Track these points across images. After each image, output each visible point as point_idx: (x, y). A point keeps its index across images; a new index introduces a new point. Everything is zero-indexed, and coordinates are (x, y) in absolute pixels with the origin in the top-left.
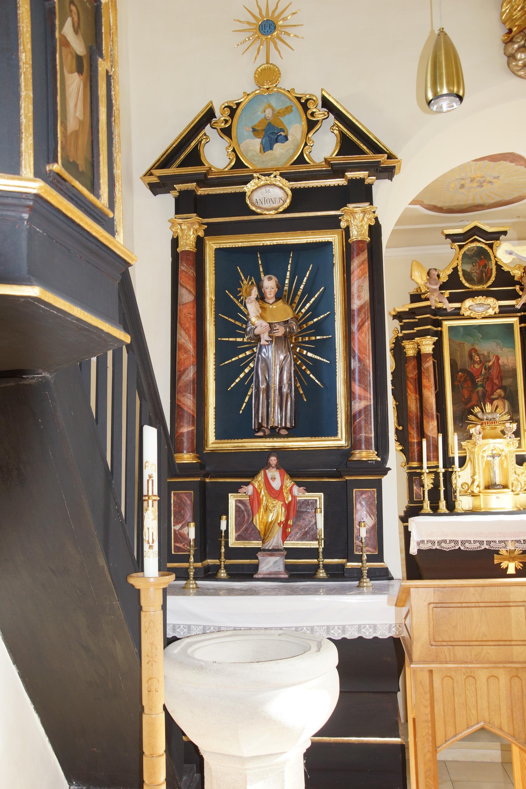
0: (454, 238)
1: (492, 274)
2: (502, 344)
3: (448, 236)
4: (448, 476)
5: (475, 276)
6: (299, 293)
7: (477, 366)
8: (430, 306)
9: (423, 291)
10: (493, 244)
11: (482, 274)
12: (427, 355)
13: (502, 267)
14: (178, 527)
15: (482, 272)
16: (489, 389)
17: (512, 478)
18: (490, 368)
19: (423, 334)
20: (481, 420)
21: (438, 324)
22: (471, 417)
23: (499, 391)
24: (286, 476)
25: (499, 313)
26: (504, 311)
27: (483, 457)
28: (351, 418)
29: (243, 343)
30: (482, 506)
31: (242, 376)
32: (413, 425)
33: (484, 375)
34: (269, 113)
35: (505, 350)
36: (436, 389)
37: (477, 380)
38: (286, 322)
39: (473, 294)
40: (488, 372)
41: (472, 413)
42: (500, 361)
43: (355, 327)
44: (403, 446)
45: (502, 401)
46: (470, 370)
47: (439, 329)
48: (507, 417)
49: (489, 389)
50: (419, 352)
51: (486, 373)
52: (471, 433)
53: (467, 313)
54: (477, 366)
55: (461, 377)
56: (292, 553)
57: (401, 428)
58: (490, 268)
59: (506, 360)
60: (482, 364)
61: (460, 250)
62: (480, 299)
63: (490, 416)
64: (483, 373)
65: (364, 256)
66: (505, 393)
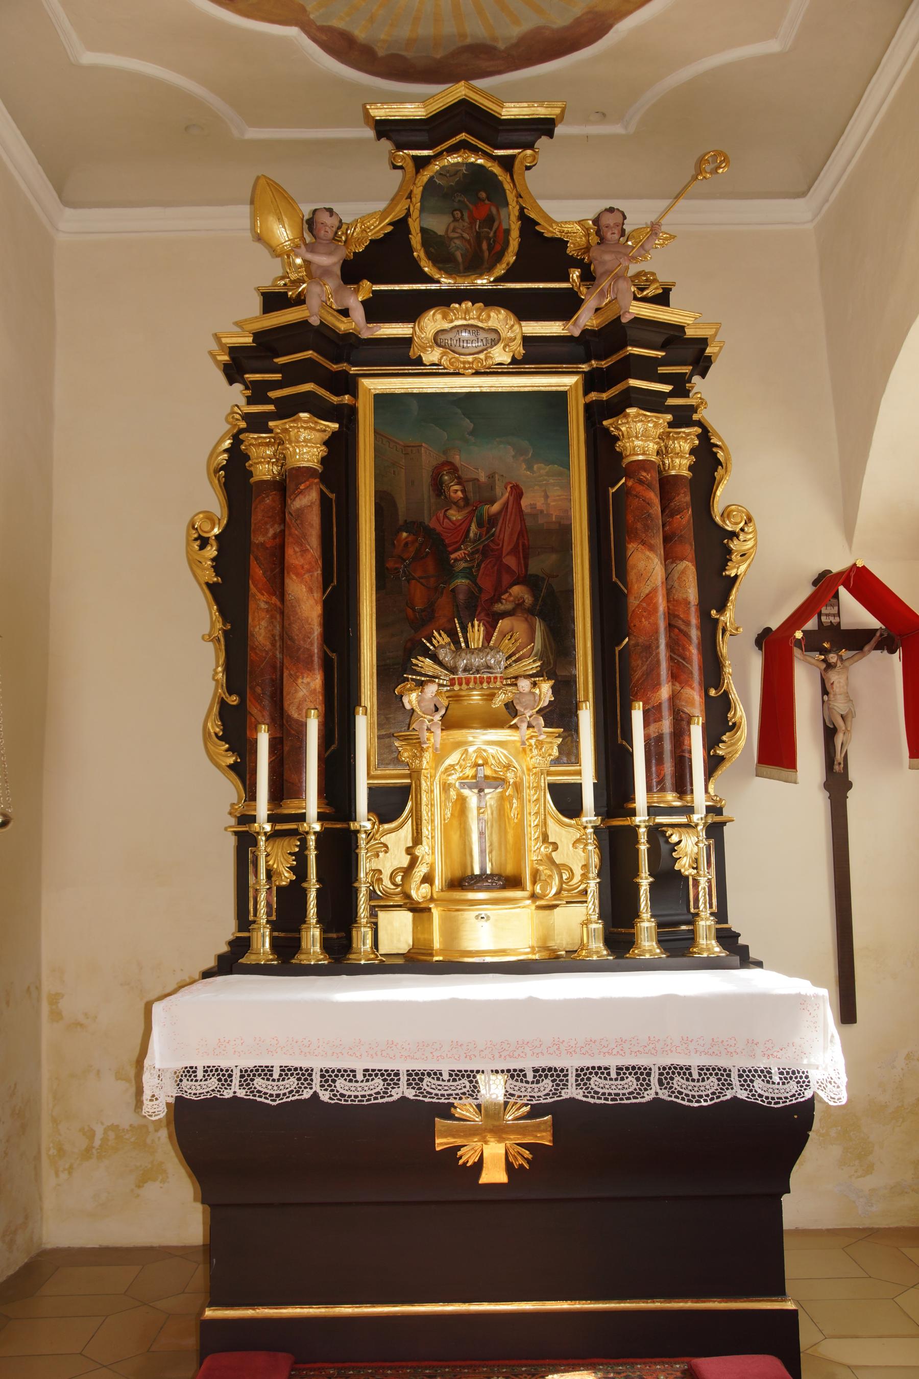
1: (507, 244)
2: (531, 452)
5: (458, 247)
7: (455, 515)
10: (513, 158)
11: (479, 245)
13: (538, 224)
15: (479, 238)
16: (486, 584)
17: (534, 852)
18: (493, 520)
23: (516, 590)
25: (526, 360)
30: (437, 945)
32: (259, 690)
33: (475, 541)
35: (541, 469)
37: (453, 556)
39: (445, 299)
40: (488, 532)
41: (426, 653)
42: (524, 502)
44: (240, 755)
45: (526, 619)
46: (433, 524)
48: (531, 665)
49: (486, 584)
51: (481, 536)
52: (408, 707)
54: (455, 515)
55: (406, 544)
57: (233, 700)
58: (505, 226)
59: (542, 500)
60: (470, 509)
61: (417, 172)
62: (467, 311)
63: (477, 661)
64: (471, 535)
66: (536, 598)
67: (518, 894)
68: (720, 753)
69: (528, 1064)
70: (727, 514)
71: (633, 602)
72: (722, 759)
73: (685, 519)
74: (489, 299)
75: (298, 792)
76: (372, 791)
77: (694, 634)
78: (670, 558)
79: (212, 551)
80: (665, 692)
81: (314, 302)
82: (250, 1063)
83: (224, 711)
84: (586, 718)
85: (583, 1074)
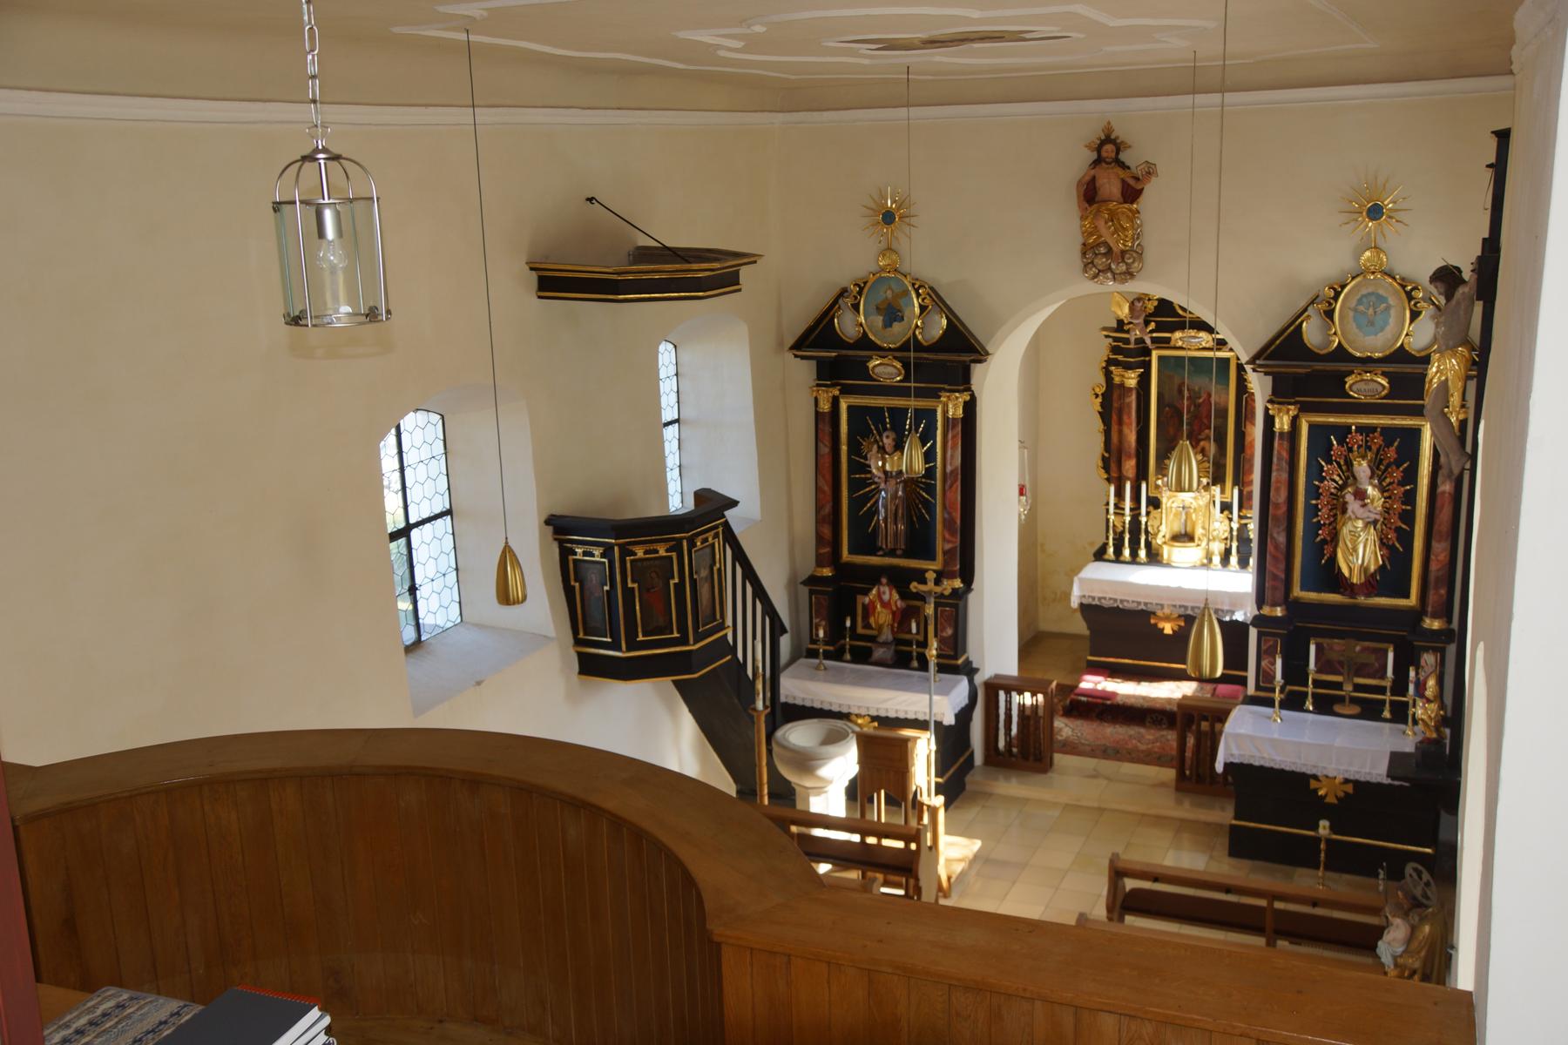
14: (818, 620)
17: (1199, 532)
18: (1199, 405)
19: (1128, 367)
21: (1147, 352)
27: (1171, 508)
28: (945, 553)
34: (889, 294)
36: (1138, 423)
43: (947, 487)
47: (1147, 359)
53: (1180, 343)
57: (1106, 455)
69: (1178, 603)
71: (1248, 439)
75: (1124, 500)
79: (1100, 400)
82: (1100, 595)
83: (1103, 456)
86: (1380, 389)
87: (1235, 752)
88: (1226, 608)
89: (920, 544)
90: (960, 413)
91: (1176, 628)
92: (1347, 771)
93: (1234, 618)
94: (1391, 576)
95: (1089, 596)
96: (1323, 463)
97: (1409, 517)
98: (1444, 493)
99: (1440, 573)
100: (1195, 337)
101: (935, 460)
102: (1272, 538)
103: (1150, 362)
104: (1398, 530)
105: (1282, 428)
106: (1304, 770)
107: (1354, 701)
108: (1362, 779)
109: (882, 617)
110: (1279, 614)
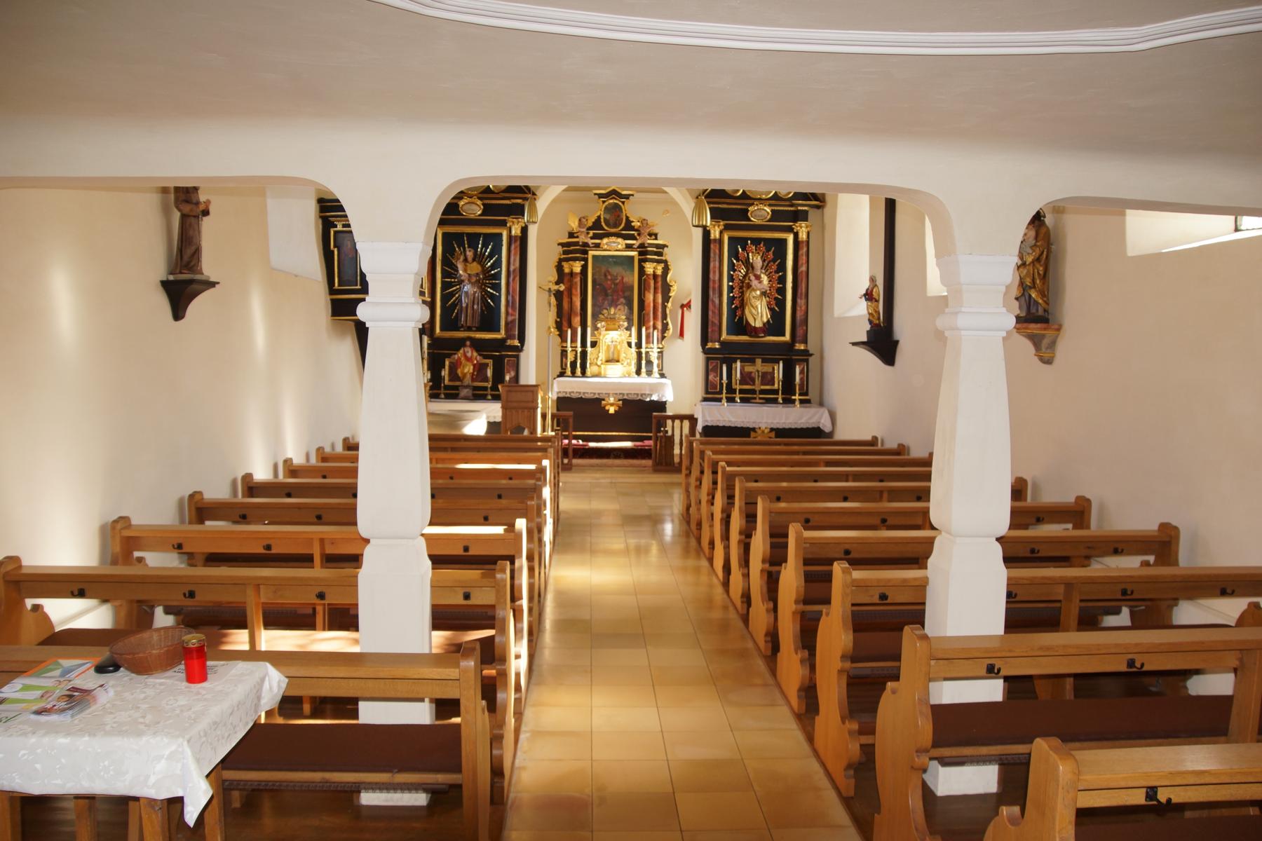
0: (600, 196)
3: (595, 194)
4: (584, 354)
5: (611, 222)
6: (485, 257)
8: (578, 242)
9: (575, 231)
12: (576, 274)
15: (616, 220)
16: (615, 297)
17: (623, 356)
18: (617, 284)
19: (575, 259)
20: (607, 318)
21: (586, 252)
22: (601, 316)
24: (474, 351)
26: (629, 247)
29: (455, 282)
31: (454, 298)
38: (477, 274)
39: (608, 235)
41: (601, 314)
42: (624, 280)
50: (572, 270)
54: (609, 282)
56: (475, 388)
57: (558, 320)
63: (612, 317)
65: (518, 243)
67: (618, 363)
68: (666, 335)
69: (618, 392)
70: (670, 281)
71: (646, 304)
72: (665, 337)
73: (659, 284)
74: (618, 235)
76: (591, 342)
77: (660, 310)
78: (655, 292)
80: (651, 323)
81: (580, 237)
82: (570, 390)
83: (556, 321)
84: (634, 330)
85: (628, 394)
86: (766, 214)
87: (709, 419)
88: (647, 392)
89: (488, 320)
90: (519, 233)
91: (617, 408)
92: (772, 423)
93: (652, 399)
94: (776, 325)
95: (564, 392)
96: (735, 261)
97: (782, 291)
98: (802, 272)
99: (803, 317)
100: (614, 242)
101: (501, 268)
102: (713, 301)
103: (587, 258)
104: (776, 299)
105: (715, 236)
106: (748, 425)
107: (760, 398)
108: (781, 427)
109: (468, 369)
110: (717, 347)
